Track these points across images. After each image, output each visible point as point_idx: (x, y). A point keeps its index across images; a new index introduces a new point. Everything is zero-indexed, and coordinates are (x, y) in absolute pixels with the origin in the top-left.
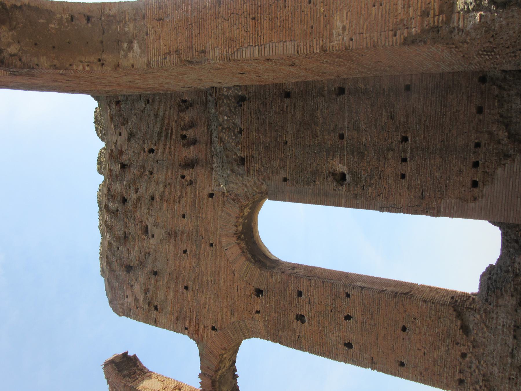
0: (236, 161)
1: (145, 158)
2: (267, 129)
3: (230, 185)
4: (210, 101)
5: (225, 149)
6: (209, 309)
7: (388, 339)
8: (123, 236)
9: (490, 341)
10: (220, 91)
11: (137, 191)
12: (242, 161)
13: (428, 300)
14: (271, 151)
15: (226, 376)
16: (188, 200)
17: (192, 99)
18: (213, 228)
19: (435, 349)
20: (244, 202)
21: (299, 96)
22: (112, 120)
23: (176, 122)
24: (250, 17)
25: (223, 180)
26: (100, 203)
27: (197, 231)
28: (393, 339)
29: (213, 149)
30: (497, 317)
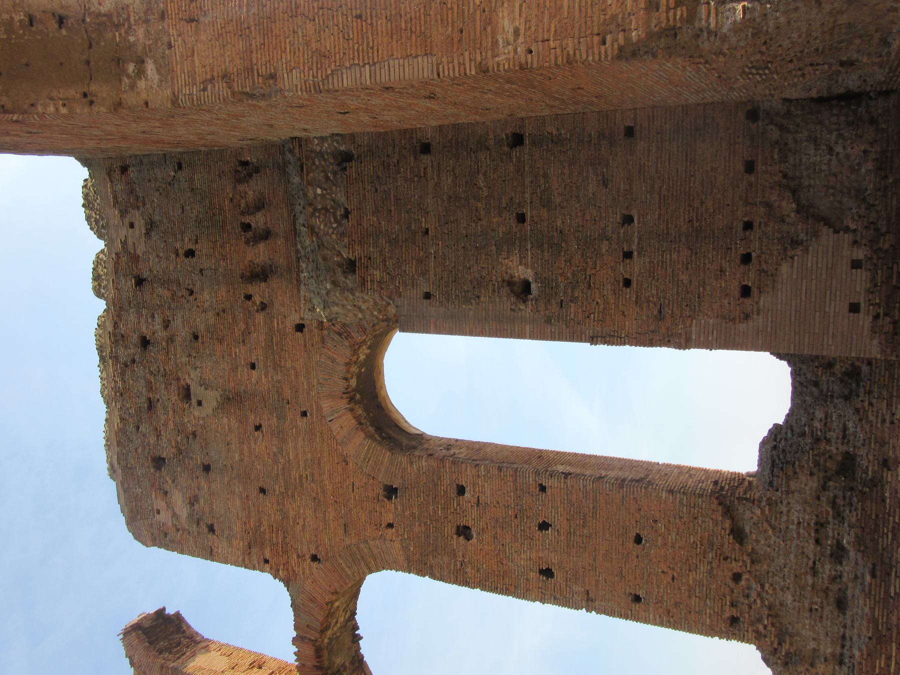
0: (340, 267)
1: (179, 266)
2: (393, 208)
5: (321, 246)
6: (304, 525)
7: (611, 558)
8: (146, 405)
9: (779, 551)
10: (306, 144)
11: (166, 325)
12: (351, 266)
13: (676, 489)
14: (401, 246)
15: (341, 638)
16: (259, 337)
17: (258, 160)
18: (305, 384)
19: (690, 570)
20: (359, 338)
22: (116, 202)
23: (231, 200)
24: (352, 14)
26: (100, 349)
27: (278, 392)
28: (620, 557)
29: (299, 247)
30: (789, 511)
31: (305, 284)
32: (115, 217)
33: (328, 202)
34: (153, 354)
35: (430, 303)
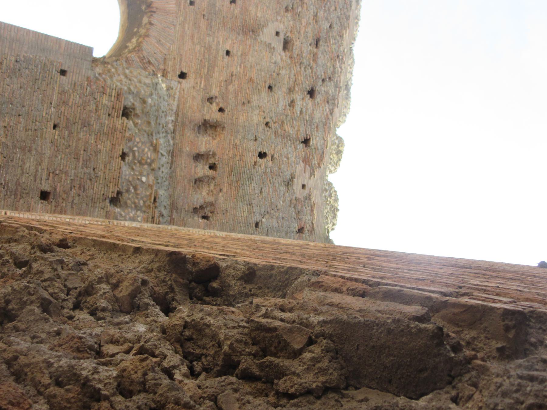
0: (137, 114)
1: (273, 147)
2: (82, 152)
3: (150, 82)
4: (165, 207)
5: (150, 135)
8: (321, 43)
10: (148, 218)
11: (292, 103)
12: (126, 113)
14: (80, 119)
16: (218, 76)
17: (193, 218)
18: (186, 28)
20: (133, 56)
21: (27, 191)
23: (221, 190)
25: (160, 92)
27: (211, 27)
29: (171, 142)
31: (172, 110)
32: (316, 195)
33: (138, 169)
34: (307, 82)
35: (62, 65)
